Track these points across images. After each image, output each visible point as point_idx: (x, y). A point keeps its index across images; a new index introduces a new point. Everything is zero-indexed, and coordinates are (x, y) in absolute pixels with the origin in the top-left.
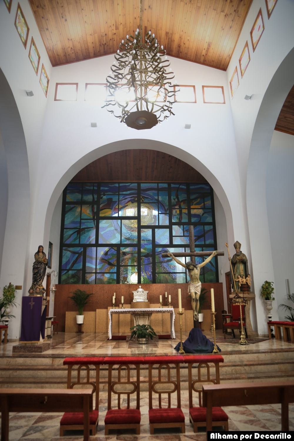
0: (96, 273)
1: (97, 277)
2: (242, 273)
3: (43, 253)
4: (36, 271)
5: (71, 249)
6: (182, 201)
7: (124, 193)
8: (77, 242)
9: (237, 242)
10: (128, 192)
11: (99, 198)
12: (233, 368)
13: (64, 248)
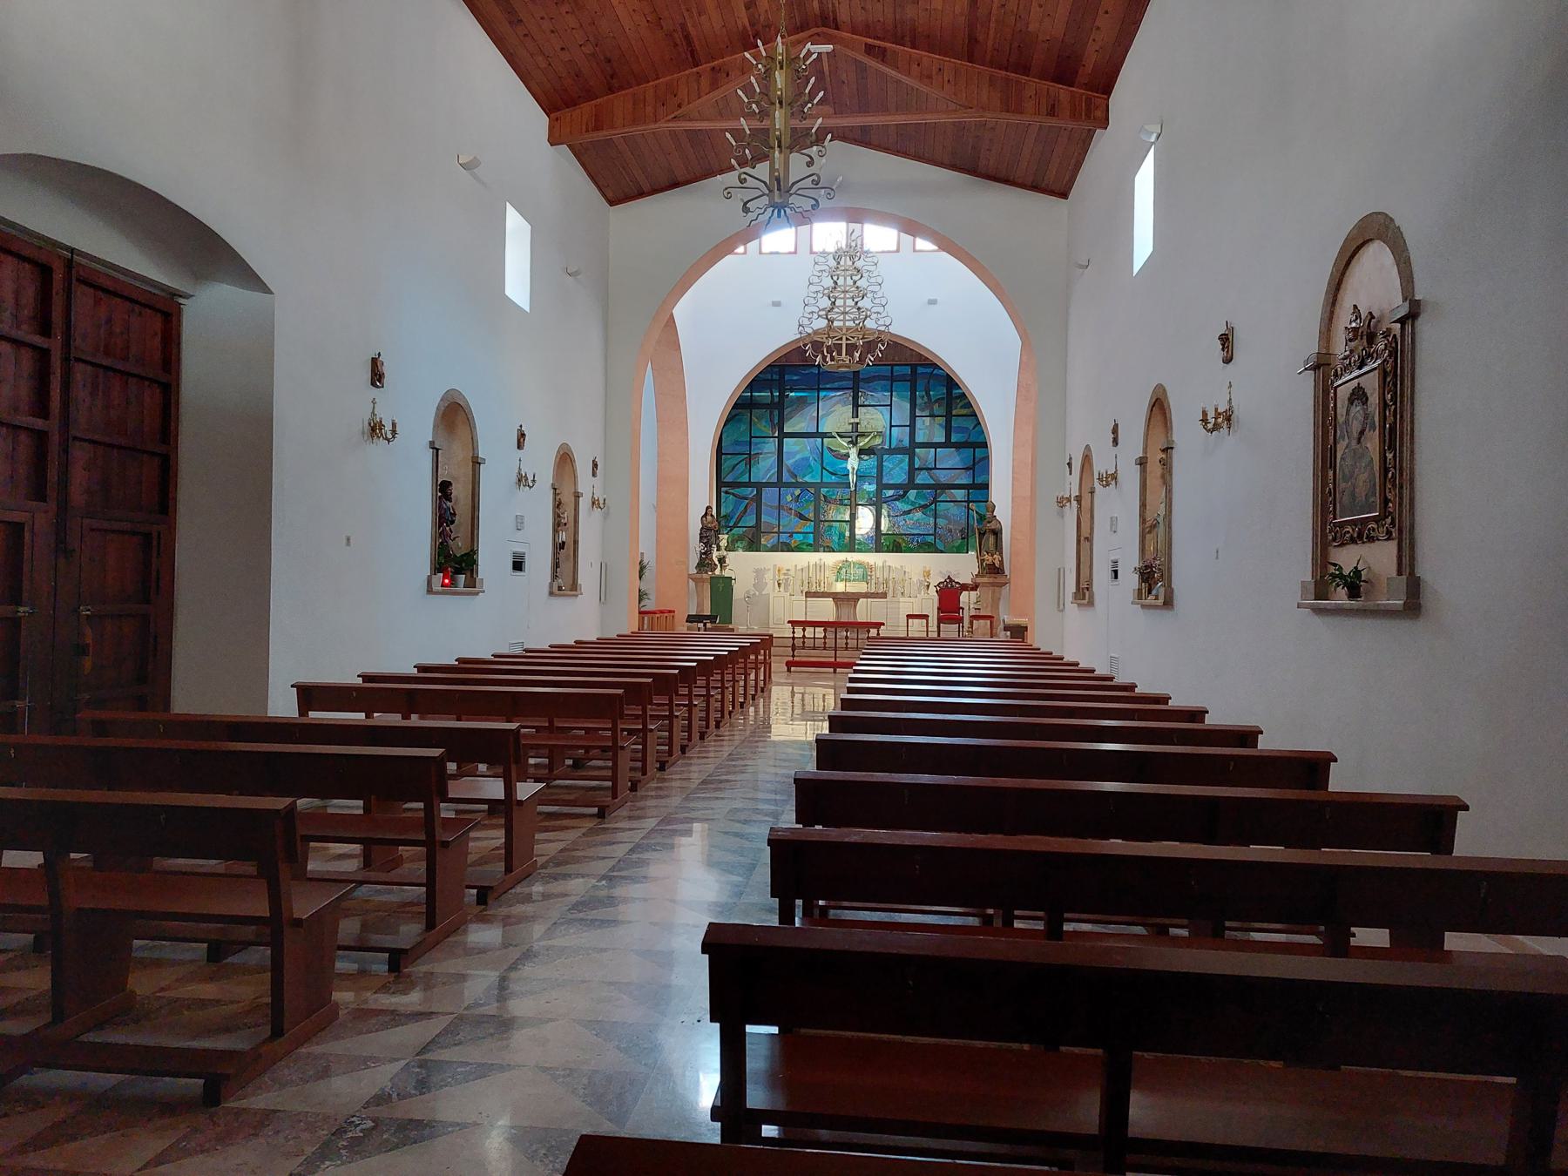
0: (779, 533)
1: (781, 540)
3: (712, 515)
4: (705, 541)
5: (736, 491)
6: (936, 401)
7: (828, 386)
8: (745, 479)
10: (836, 385)
11: (782, 396)
13: (723, 489)
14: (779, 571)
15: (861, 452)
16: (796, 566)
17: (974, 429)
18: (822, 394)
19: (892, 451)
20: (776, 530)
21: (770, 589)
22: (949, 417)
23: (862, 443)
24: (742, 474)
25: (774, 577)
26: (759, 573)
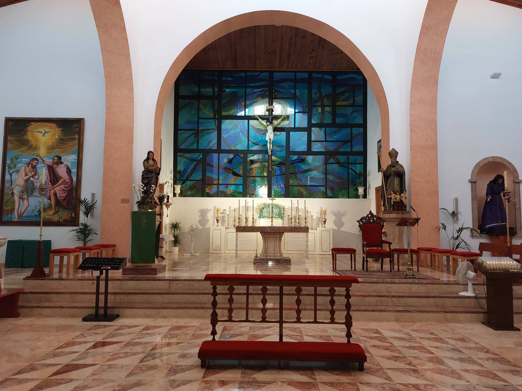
0: (218, 184)
1: (220, 190)
2: (397, 188)
3: (153, 160)
5: (188, 155)
6: (325, 96)
7: (252, 85)
8: (194, 147)
9: (393, 149)
10: (258, 84)
11: (221, 91)
12: (378, 298)
13: (179, 154)
14: (217, 210)
15: (276, 129)
16: (230, 207)
17: (351, 114)
18: (248, 90)
19: (296, 129)
20: (216, 182)
21: (211, 224)
22: (334, 107)
23: (275, 122)
24: (192, 144)
25: (214, 215)
26: (203, 213)
